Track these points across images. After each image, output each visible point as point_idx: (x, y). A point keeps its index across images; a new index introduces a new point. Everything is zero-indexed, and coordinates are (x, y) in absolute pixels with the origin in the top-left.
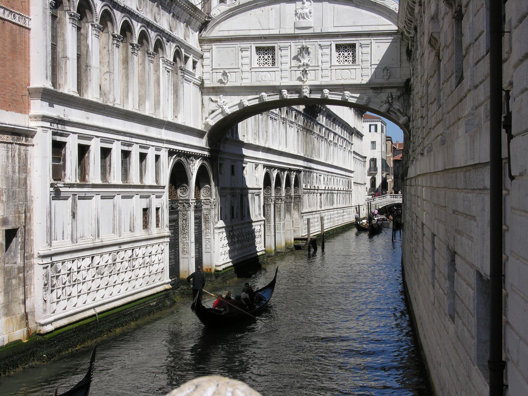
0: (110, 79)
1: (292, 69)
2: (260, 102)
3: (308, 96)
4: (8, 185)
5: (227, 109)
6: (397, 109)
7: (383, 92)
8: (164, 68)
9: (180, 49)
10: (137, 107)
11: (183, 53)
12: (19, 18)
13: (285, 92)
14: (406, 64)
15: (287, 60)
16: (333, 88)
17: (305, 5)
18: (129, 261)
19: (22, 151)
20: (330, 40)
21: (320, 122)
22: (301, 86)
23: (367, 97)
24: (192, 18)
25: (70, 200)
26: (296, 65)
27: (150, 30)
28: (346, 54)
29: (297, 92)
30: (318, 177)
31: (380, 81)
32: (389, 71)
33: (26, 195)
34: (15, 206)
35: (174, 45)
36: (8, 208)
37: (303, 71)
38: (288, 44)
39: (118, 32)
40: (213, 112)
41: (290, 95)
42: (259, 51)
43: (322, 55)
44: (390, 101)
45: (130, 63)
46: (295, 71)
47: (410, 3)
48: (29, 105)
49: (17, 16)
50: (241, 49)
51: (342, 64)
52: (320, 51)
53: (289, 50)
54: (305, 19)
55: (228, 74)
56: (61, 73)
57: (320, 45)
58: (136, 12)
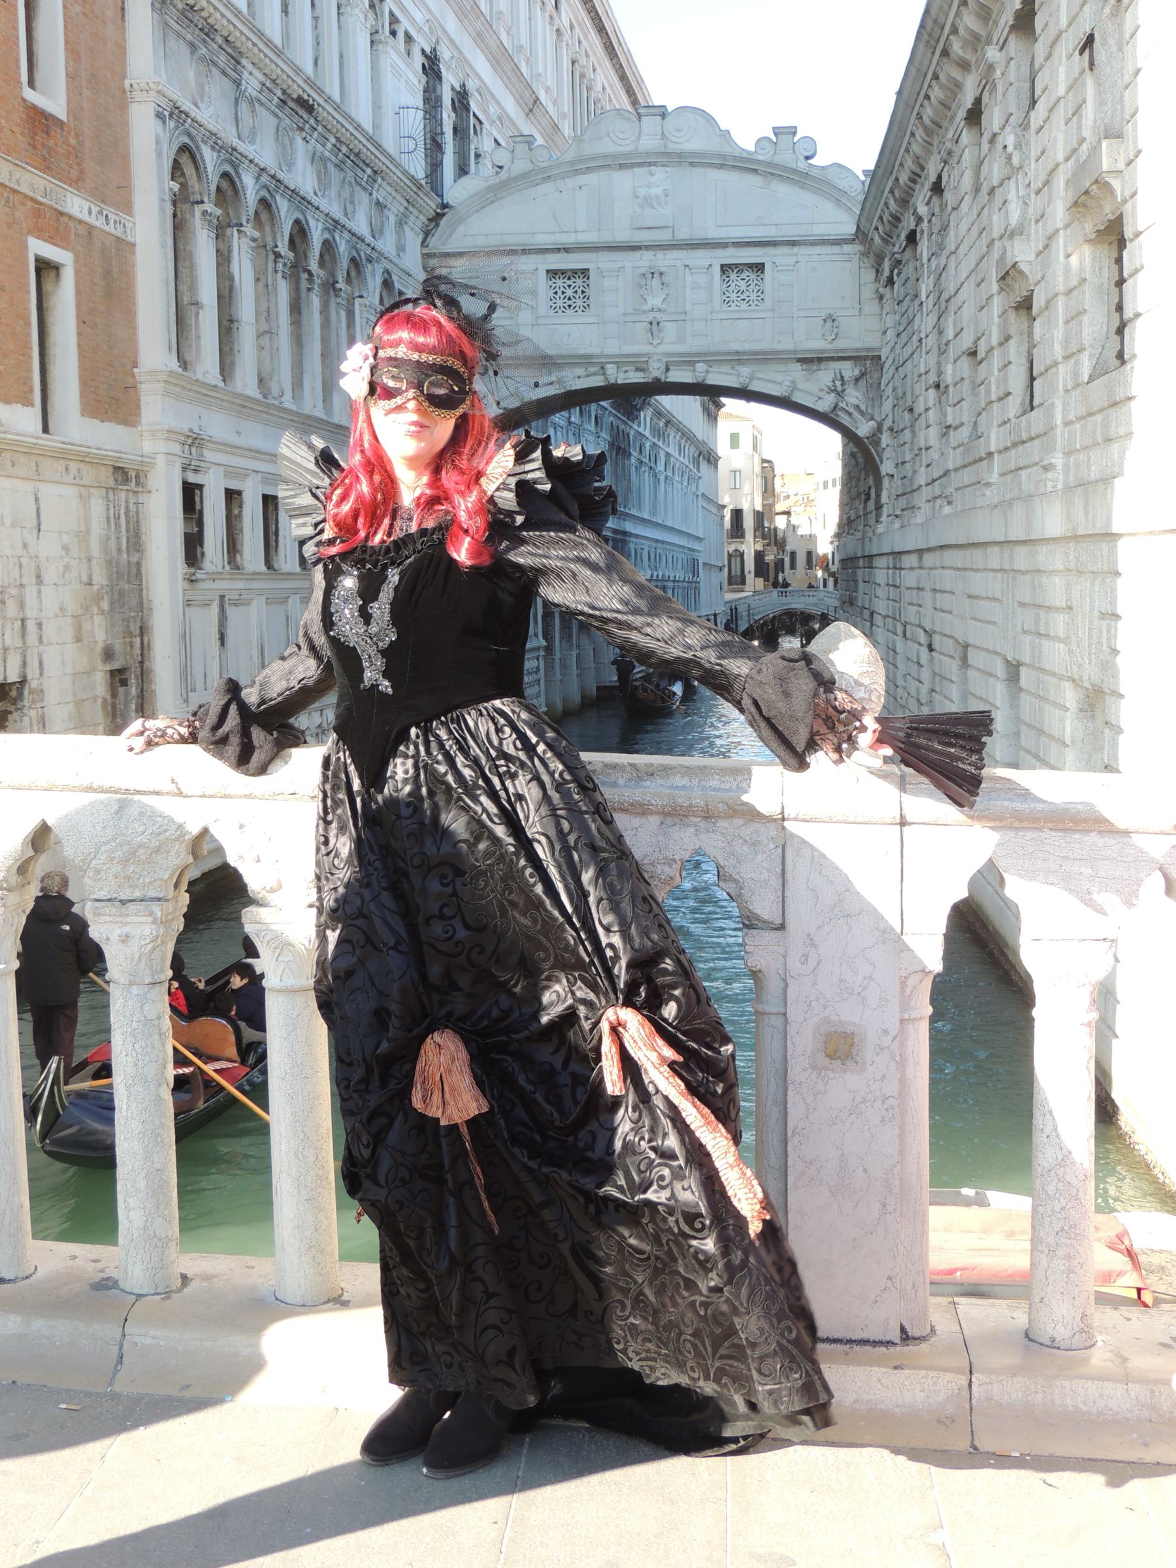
0: (271, 347)
2: (557, 392)
3: (663, 379)
4: (110, 577)
8: (364, 321)
9: (391, 277)
10: (320, 404)
11: (397, 286)
12: (115, 222)
13: (611, 369)
14: (872, 307)
16: (714, 358)
17: (653, 179)
18: (317, 735)
19: (131, 506)
21: (641, 430)
22: (649, 355)
24: (411, 208)
25: (215, 608)
27: (337, 238)
28: (743, 285)
29: (638, 369)
30: (639, 551)
32: (836, 324)
33: (141, 597)
34: (123, 620)
35: (379, 269)
36: (113, 626)
38: (617, 265)
39: (283, 248)
44: (839, 388)
45: (304, 311)
47: (904, 178)
48: (138, 407)
49: (112, 217)
52: (689, 279)
56: (187, 338)
58: (316, 201)
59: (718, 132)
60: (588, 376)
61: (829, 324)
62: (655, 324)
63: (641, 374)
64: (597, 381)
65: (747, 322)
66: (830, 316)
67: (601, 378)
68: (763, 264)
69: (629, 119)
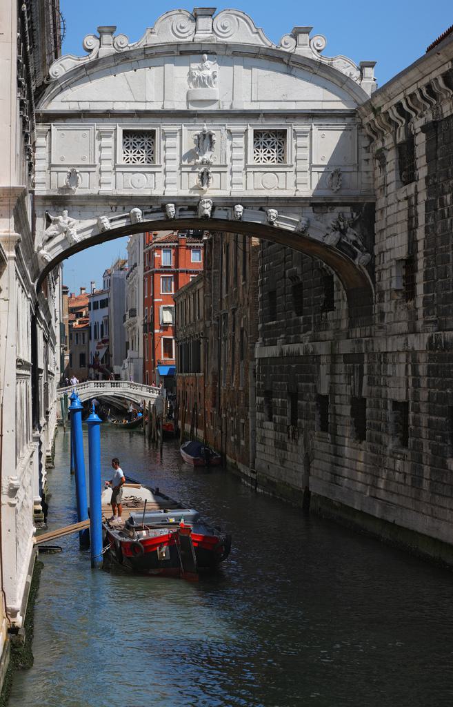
1: (183, 169)
2: (130, 224)
3: (210, 216)
5: (75, 233)
6: (351, 241)
7: (329, 211)
15: (175, 153)
22: (200, 198)
23: (307, 219)
31: (326, 193)
32: (341, 178)
37: (203, 173)
38: (177, 128)
41: (178, 212)
42: (127, 138)
44: (342, 227)
46: (189, 172)
51: (261, 163)
52: (229, 143)
53: (178, 137)
54: (206, 86)
57: (229, 131)
59: (255, 30)
60: (152, 212)
61: (335, 178)
62: (205, 174)
63: (192, 213)
64: (159, 216)
66: (336, 172)
67: (162, 214)
68: (286, 130)
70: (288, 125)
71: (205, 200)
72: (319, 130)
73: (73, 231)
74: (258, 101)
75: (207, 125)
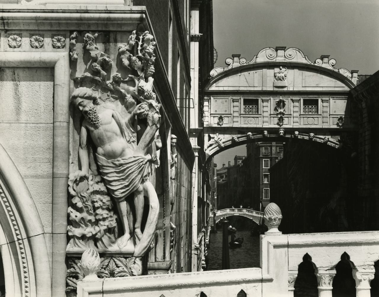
3: (283, 136)
13: (266, 132)
17: (281, 71)
20: (300, 96)
22: (279, 128)
26: (274, 113)
28: (310, 107)
37: (280, 118)
38: (268, 98)
40: (211, 145)
43: (294, 107)
46: (274, 117)
50: (233, 100)
51: (307, 114)
52: (292, 103)
55: (223, 118)
59: (304, 56)
65: (312, 118)
67: (262, 135)
69: (273, 51)
70: (319, 97)
71: (282, 129)
72: (333, 99)
73: (221, 142)
74: (305, 87)
75: (282, 97)
